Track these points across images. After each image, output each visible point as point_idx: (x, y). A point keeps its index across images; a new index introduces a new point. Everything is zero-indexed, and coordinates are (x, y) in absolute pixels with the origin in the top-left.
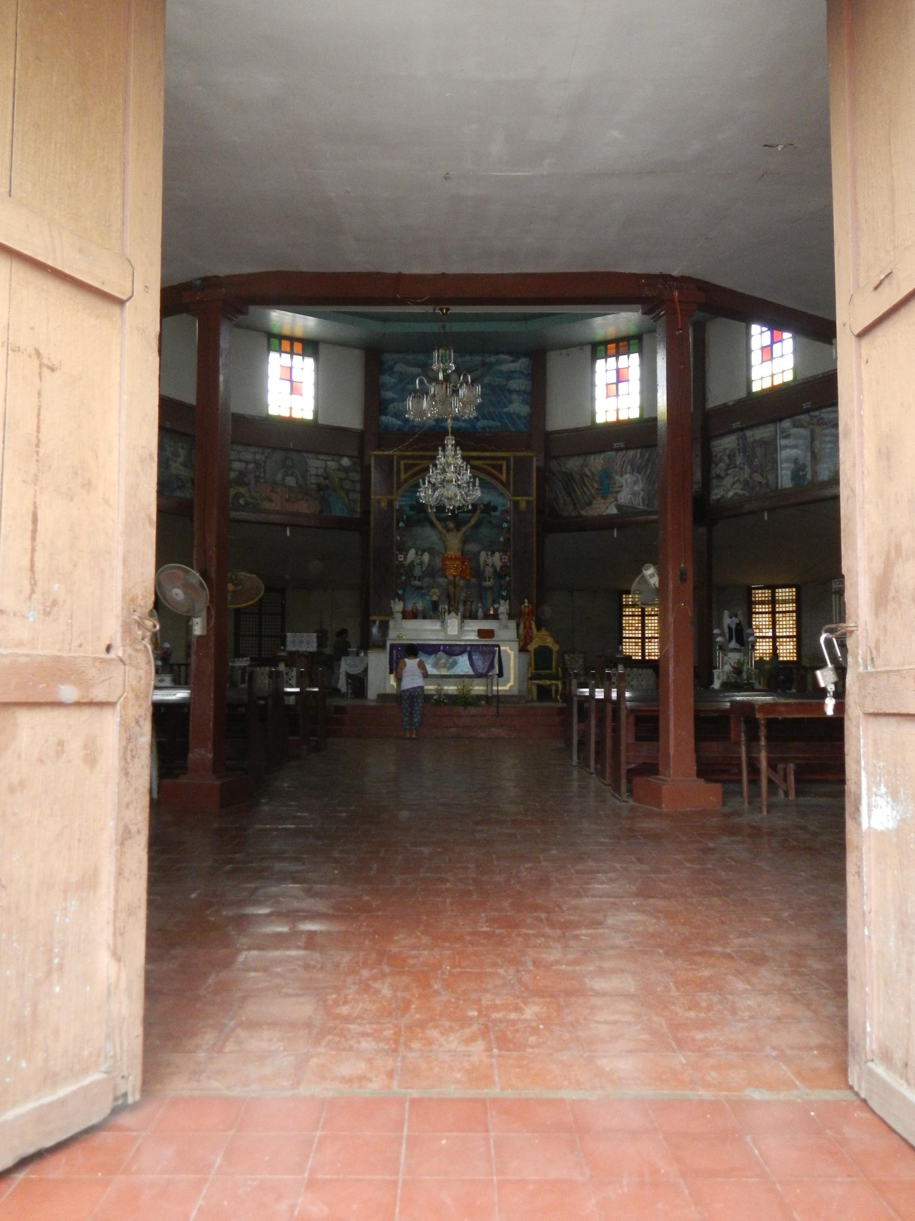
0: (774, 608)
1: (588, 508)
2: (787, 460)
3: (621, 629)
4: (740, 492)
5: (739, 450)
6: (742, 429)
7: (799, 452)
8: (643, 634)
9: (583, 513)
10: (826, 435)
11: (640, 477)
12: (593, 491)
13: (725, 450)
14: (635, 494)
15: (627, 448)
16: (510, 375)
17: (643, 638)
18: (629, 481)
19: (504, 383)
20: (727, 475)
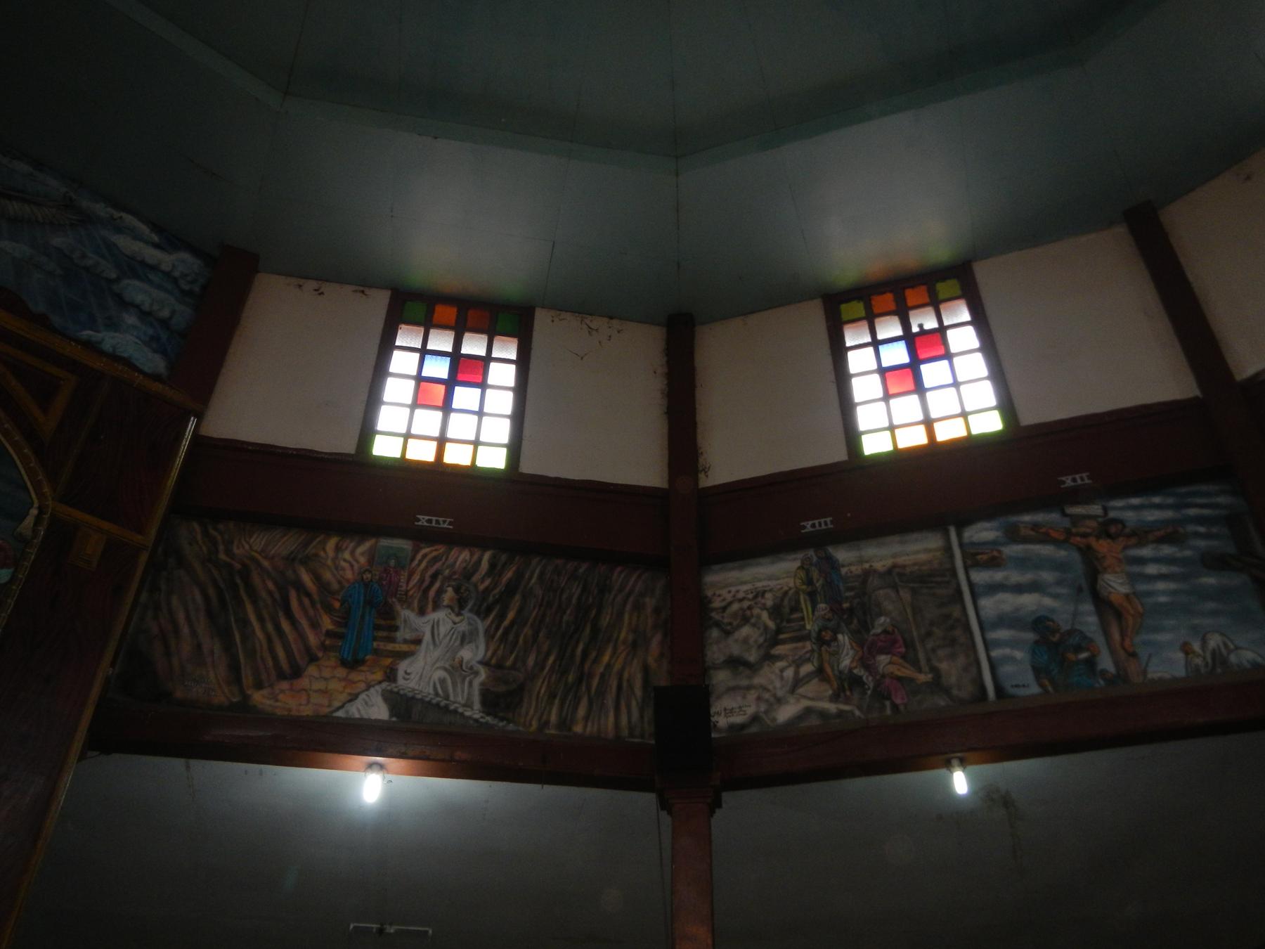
1: (285, 685)
2: (1004, 621)
4: (832, 707)
5: (812, 595)
6: (820, 541)
7: (1048, 601)
9: (259, 698)
10: (1142, 561)
11: (481, 626)
12: (313, 639)
13: (762, 593)
14: (458, 670)
15: (450, 539)
16: (136, 268)
18: (443, 630)
19: (114, 276)
20: (769, 658)
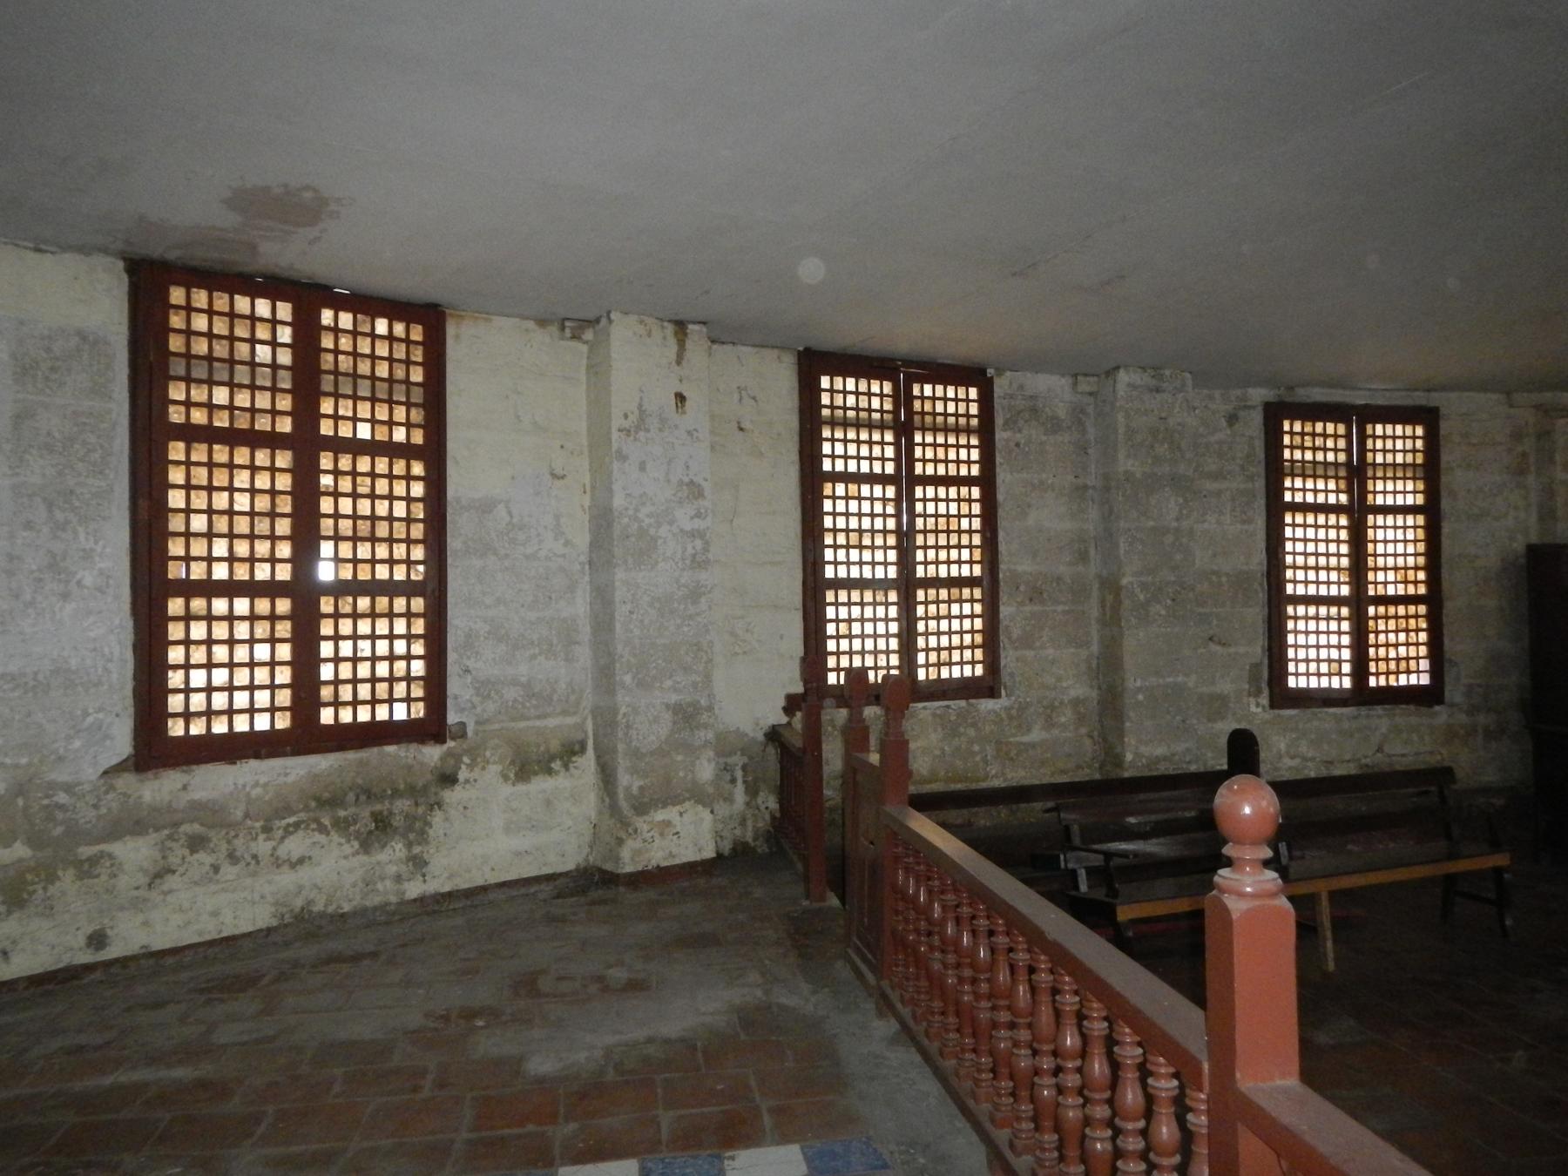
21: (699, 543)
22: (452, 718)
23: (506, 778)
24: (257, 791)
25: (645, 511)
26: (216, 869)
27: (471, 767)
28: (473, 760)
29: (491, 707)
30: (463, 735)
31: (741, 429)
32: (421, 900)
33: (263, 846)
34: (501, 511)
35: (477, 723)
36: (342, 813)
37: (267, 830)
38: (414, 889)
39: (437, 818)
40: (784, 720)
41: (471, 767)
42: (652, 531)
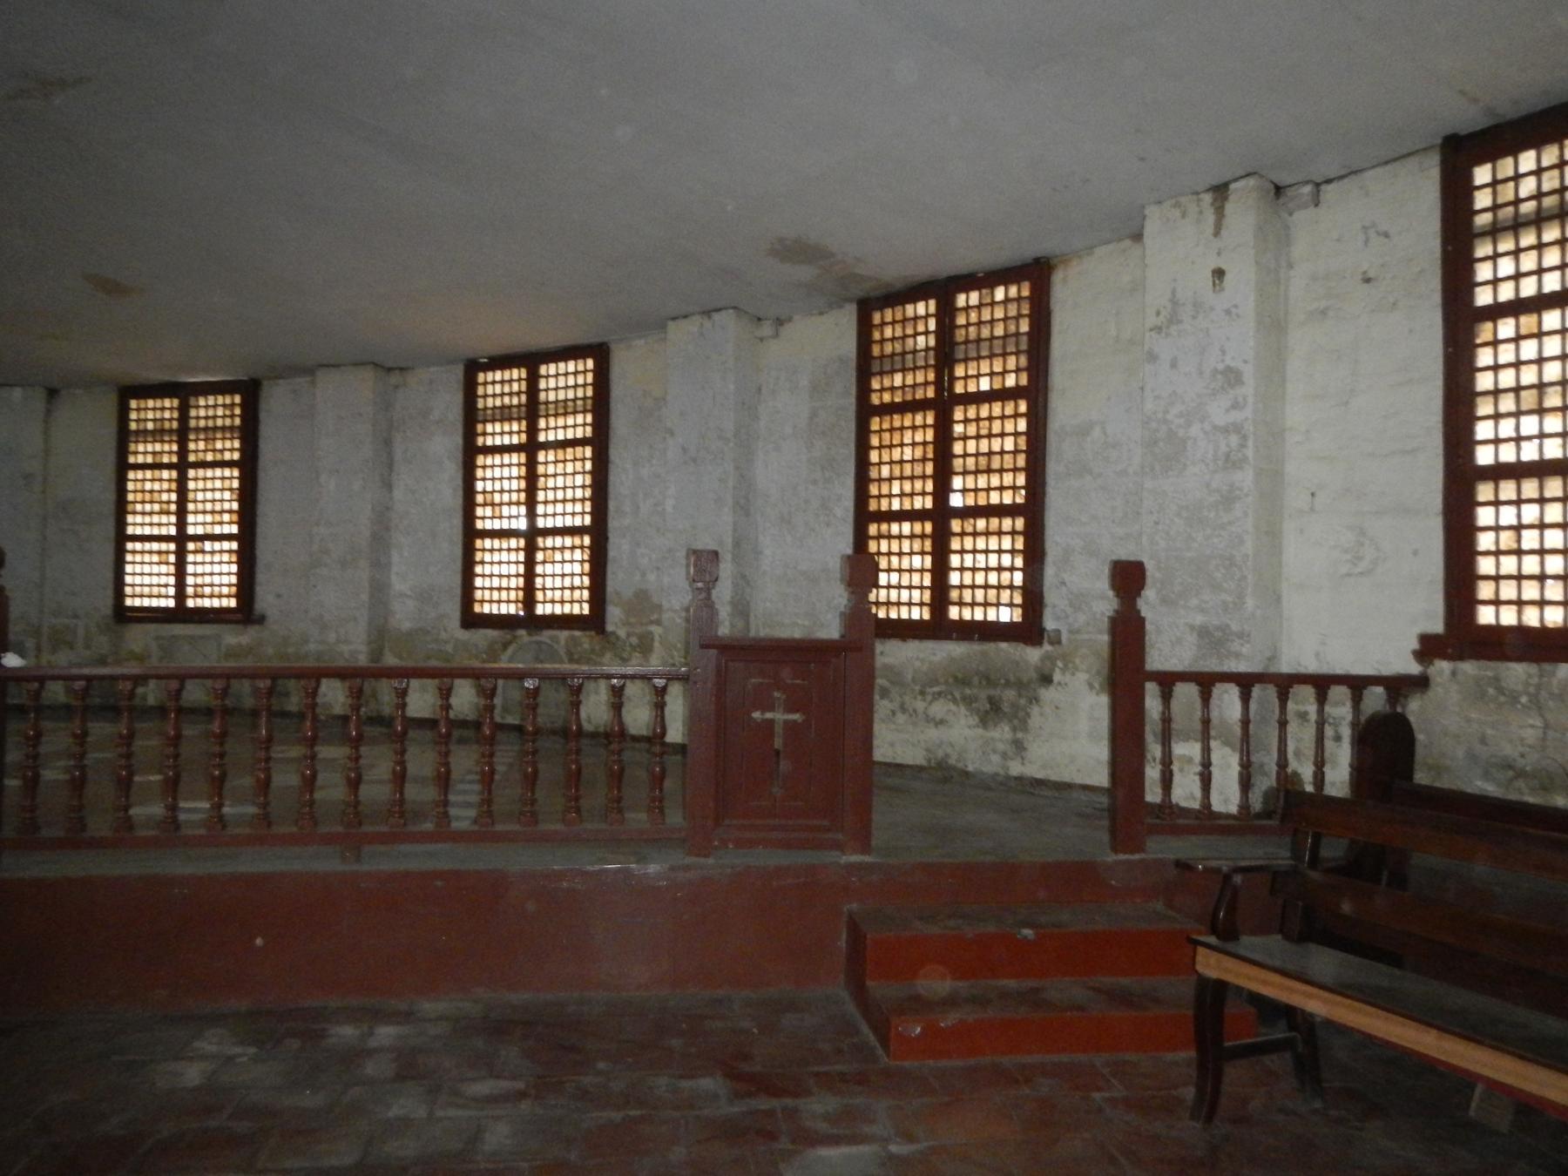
0: (532, 430)
3: (121, 508)
8: (181, 524)
17: (181, 539)
21: (1234, 440)
22: (1049, 624)
23: (1091, 686)
24: (918, 664)
25: (1174, 411)
26: (894, 713)
27: (1063, 671)
28: (1066, 665)
29: (1082, 618)
30: (1059, 642)
31: (1368, 281)
32: (1020, 779)
33: (920, 705)
34: (1097, 432)
35: (1070, 632)
36: (968, 691)
37: (922, 693)
38: (1016, 769)
39: (1035, 710)
40: (1414, 668)
41: (1063, 671)
42: (1181, 433)
